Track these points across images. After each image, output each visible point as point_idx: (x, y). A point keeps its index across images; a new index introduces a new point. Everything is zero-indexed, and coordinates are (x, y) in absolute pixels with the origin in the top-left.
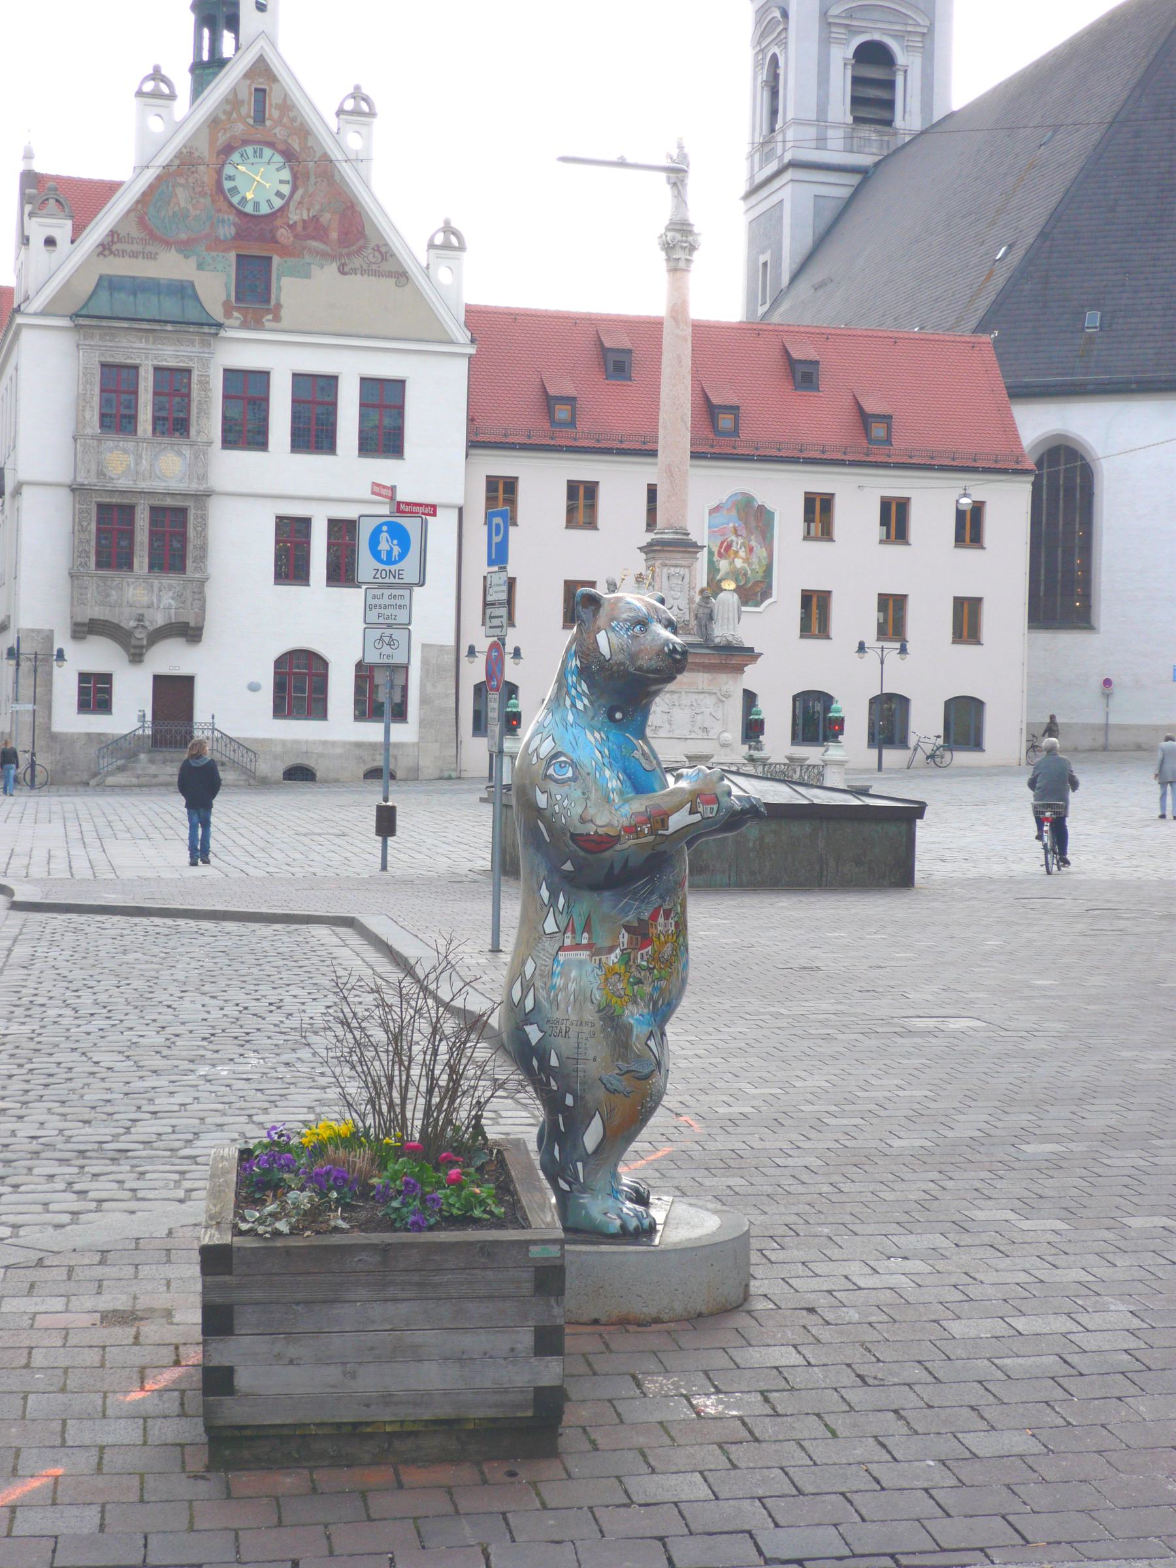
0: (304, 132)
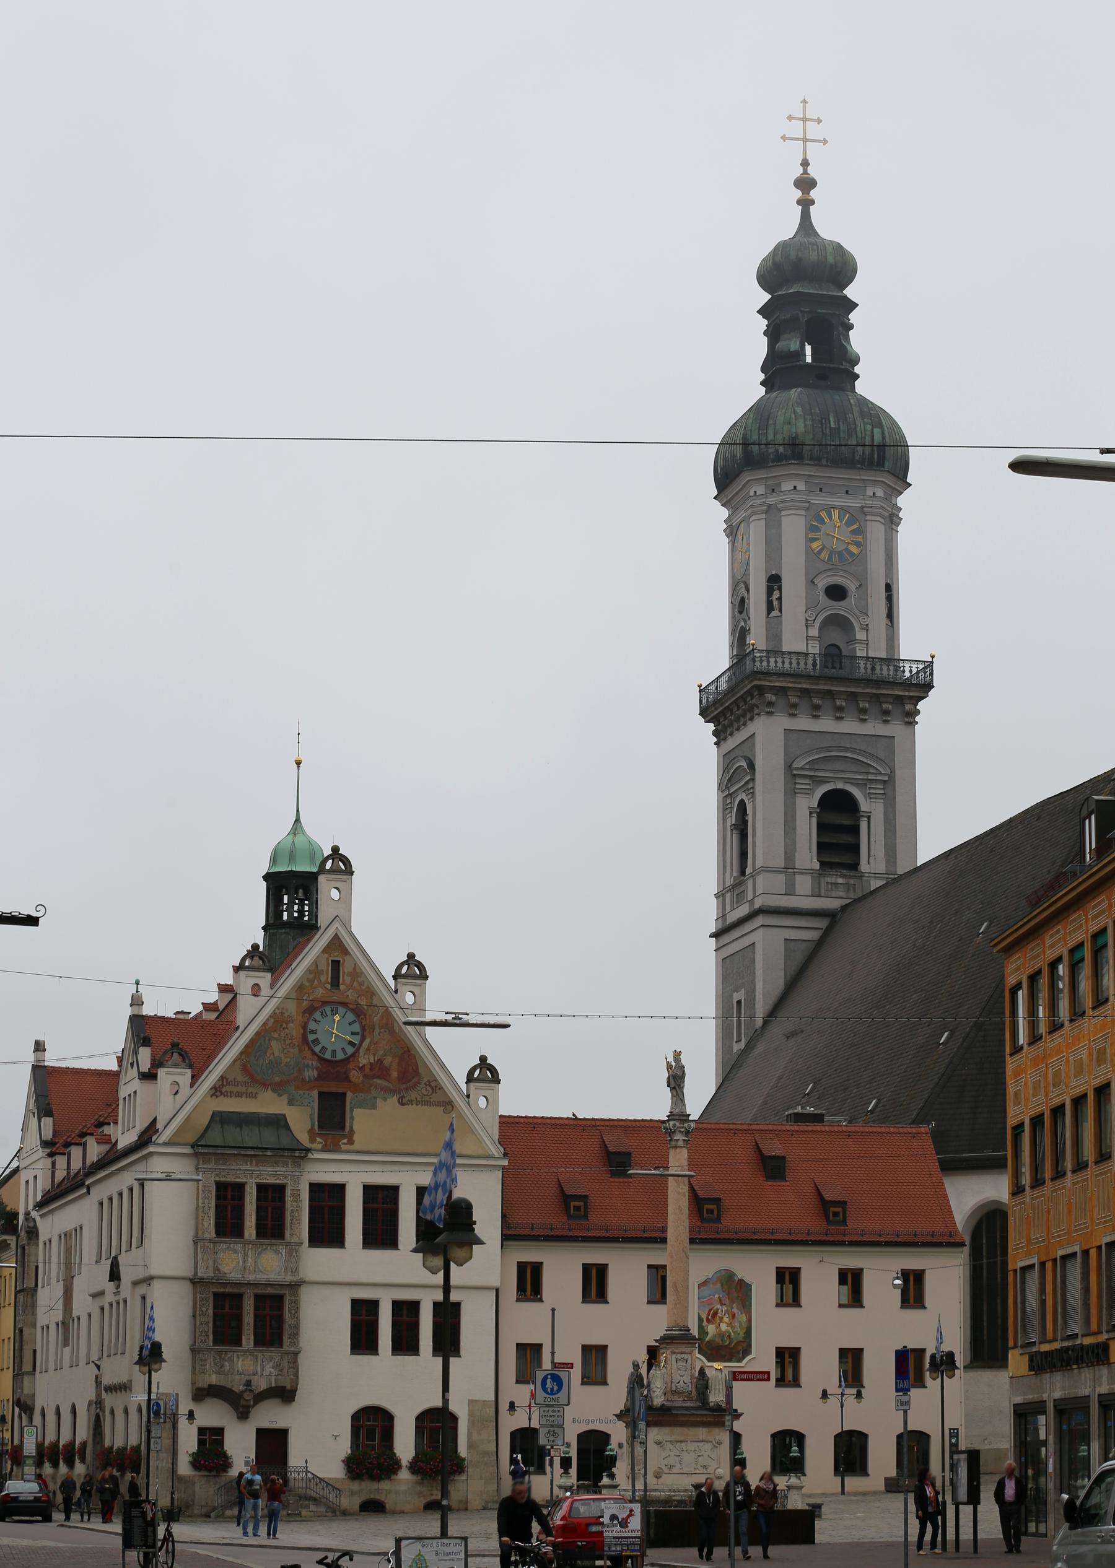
0: (371, 993)
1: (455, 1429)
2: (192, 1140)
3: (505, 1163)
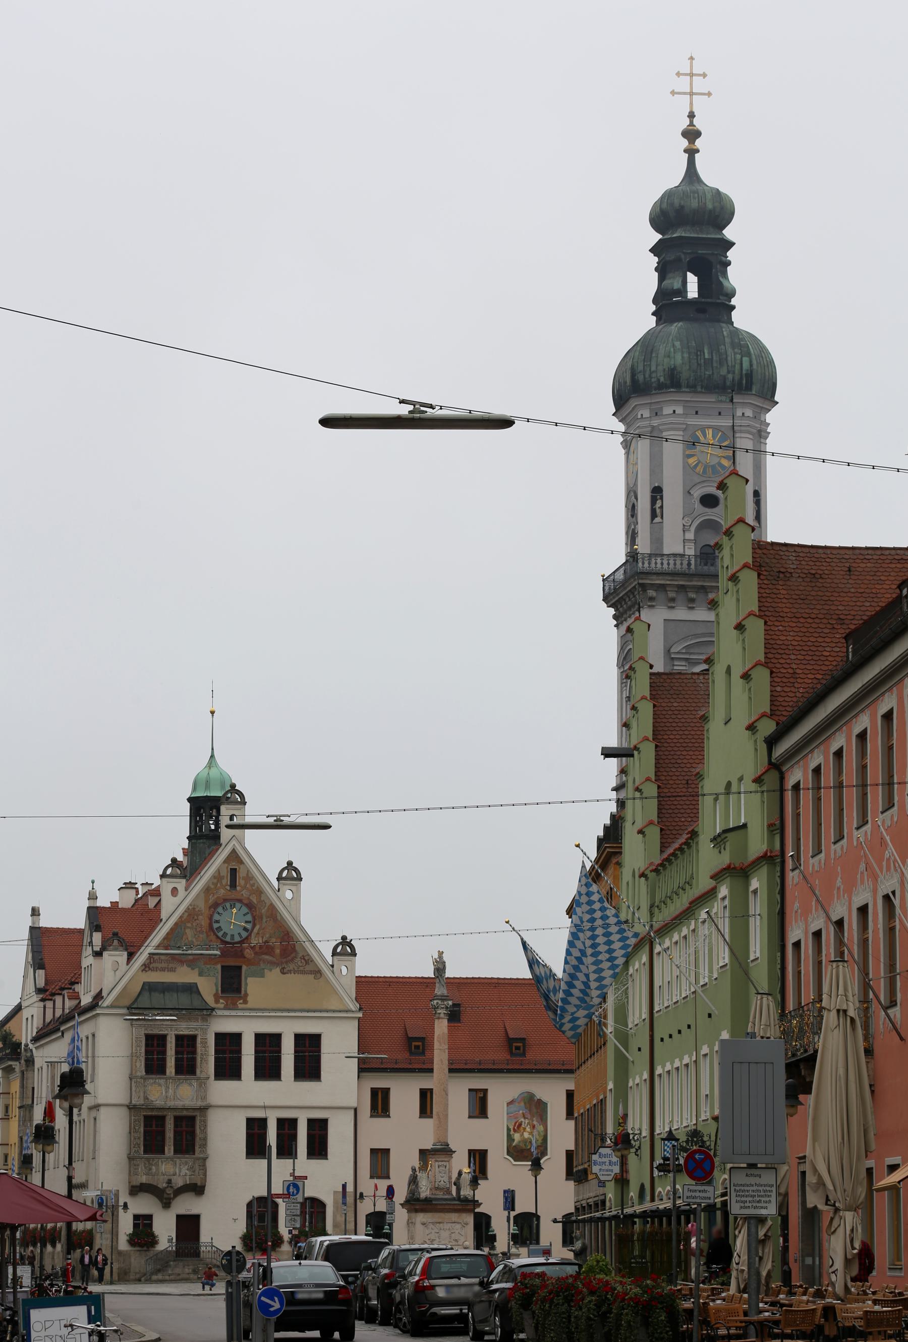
0: (260, 892)
1: (324, 1213)
2: (127, 1003)
3: (360, 1015)
